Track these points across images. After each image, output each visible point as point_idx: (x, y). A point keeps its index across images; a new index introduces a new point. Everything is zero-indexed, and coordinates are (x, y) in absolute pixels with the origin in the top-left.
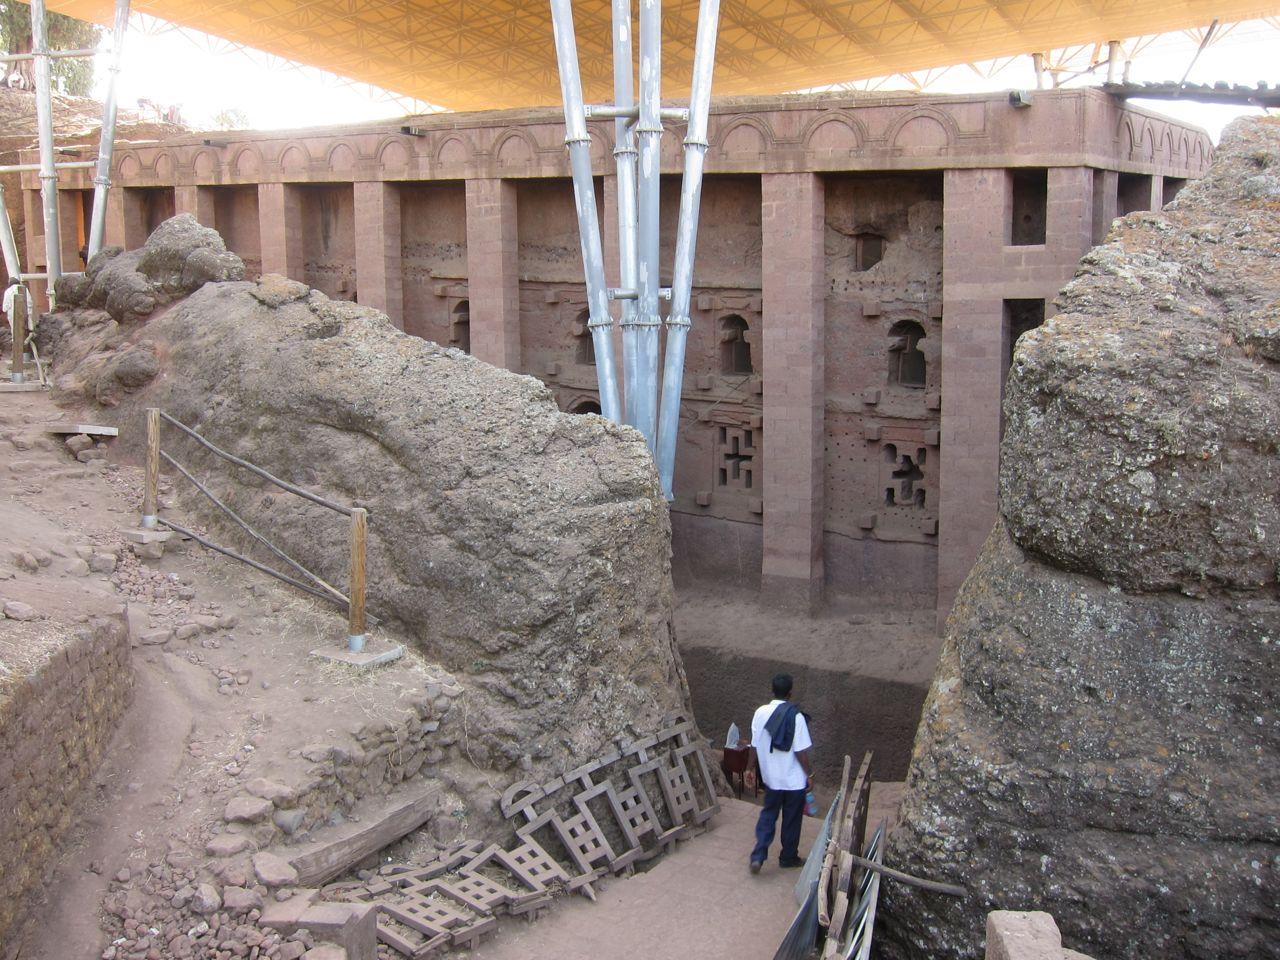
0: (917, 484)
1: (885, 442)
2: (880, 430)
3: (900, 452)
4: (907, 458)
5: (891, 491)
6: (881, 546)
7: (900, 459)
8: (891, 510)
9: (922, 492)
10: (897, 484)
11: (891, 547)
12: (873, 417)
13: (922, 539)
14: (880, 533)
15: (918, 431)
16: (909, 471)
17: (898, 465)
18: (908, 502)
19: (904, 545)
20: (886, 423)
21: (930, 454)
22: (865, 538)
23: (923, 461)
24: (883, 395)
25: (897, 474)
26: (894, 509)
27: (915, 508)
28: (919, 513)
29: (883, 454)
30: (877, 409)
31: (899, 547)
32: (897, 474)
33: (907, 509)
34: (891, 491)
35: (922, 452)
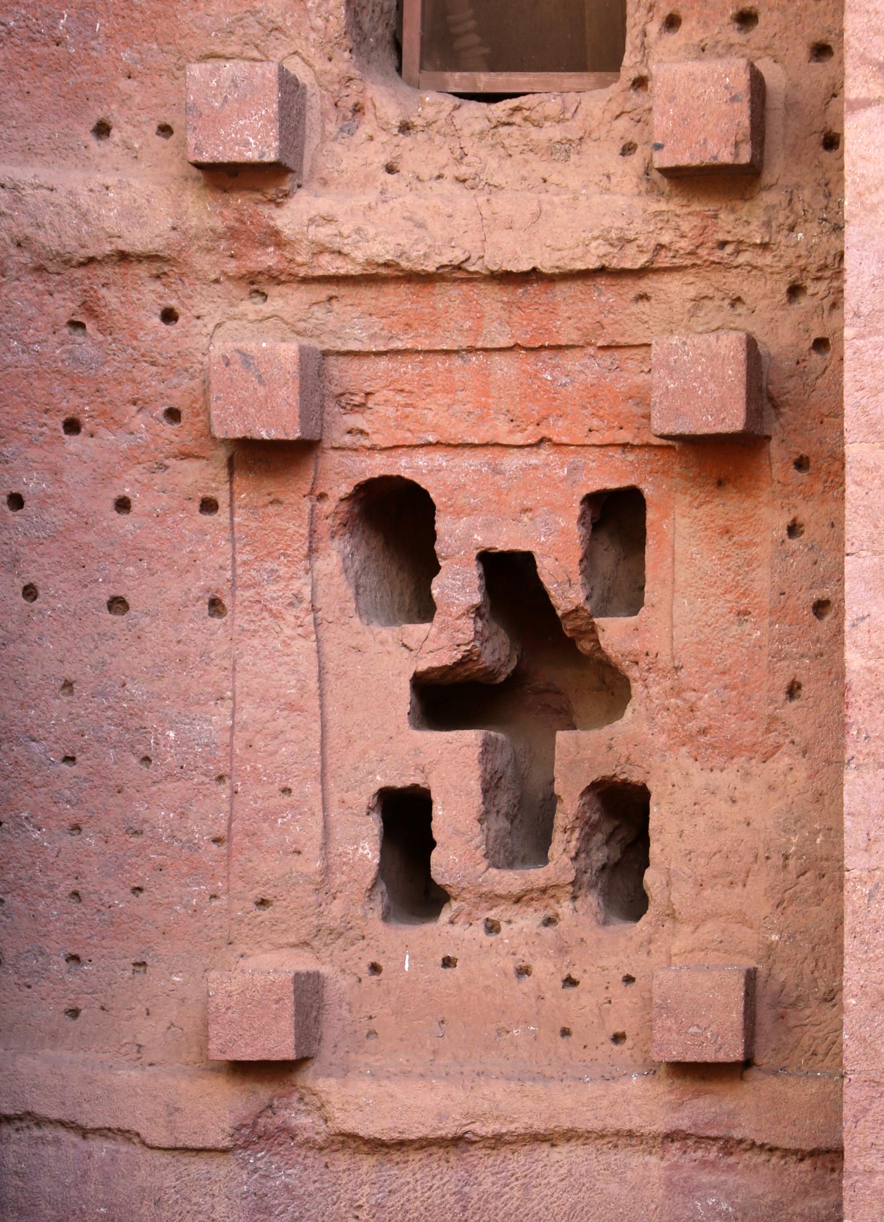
0: (578, 756)
1: (343, 473)
2: (315, 367)
3: (460, 538)
4: (509, 577)
5: (405, 816)
6: (362, 1176)
7: (458, 586)
8: (411, 946)
9: (623, 807)
10: (453, 765)
11: (415, 1178)
12: (256, 283)
13: (646, 1103)
14: (353, 1097)
15: (581, 368)
16: (526, 664)
17: (453, 628)
18: (537, 876)
19: (518, 1161)
20: (354, 323)
21: (681, 531)
22: (252, 1136)
23: (628, 595)
24: (316, 102)
25: (442, 700)
26: (446, 931)
27: (579, 914)
28: (620, 946)
29: (337, 561)
30: (295, 215)
31: (487, 1173)
32: (442, 700)
33: (526, 921)
34: (405, 816)
35: (616, 518)
